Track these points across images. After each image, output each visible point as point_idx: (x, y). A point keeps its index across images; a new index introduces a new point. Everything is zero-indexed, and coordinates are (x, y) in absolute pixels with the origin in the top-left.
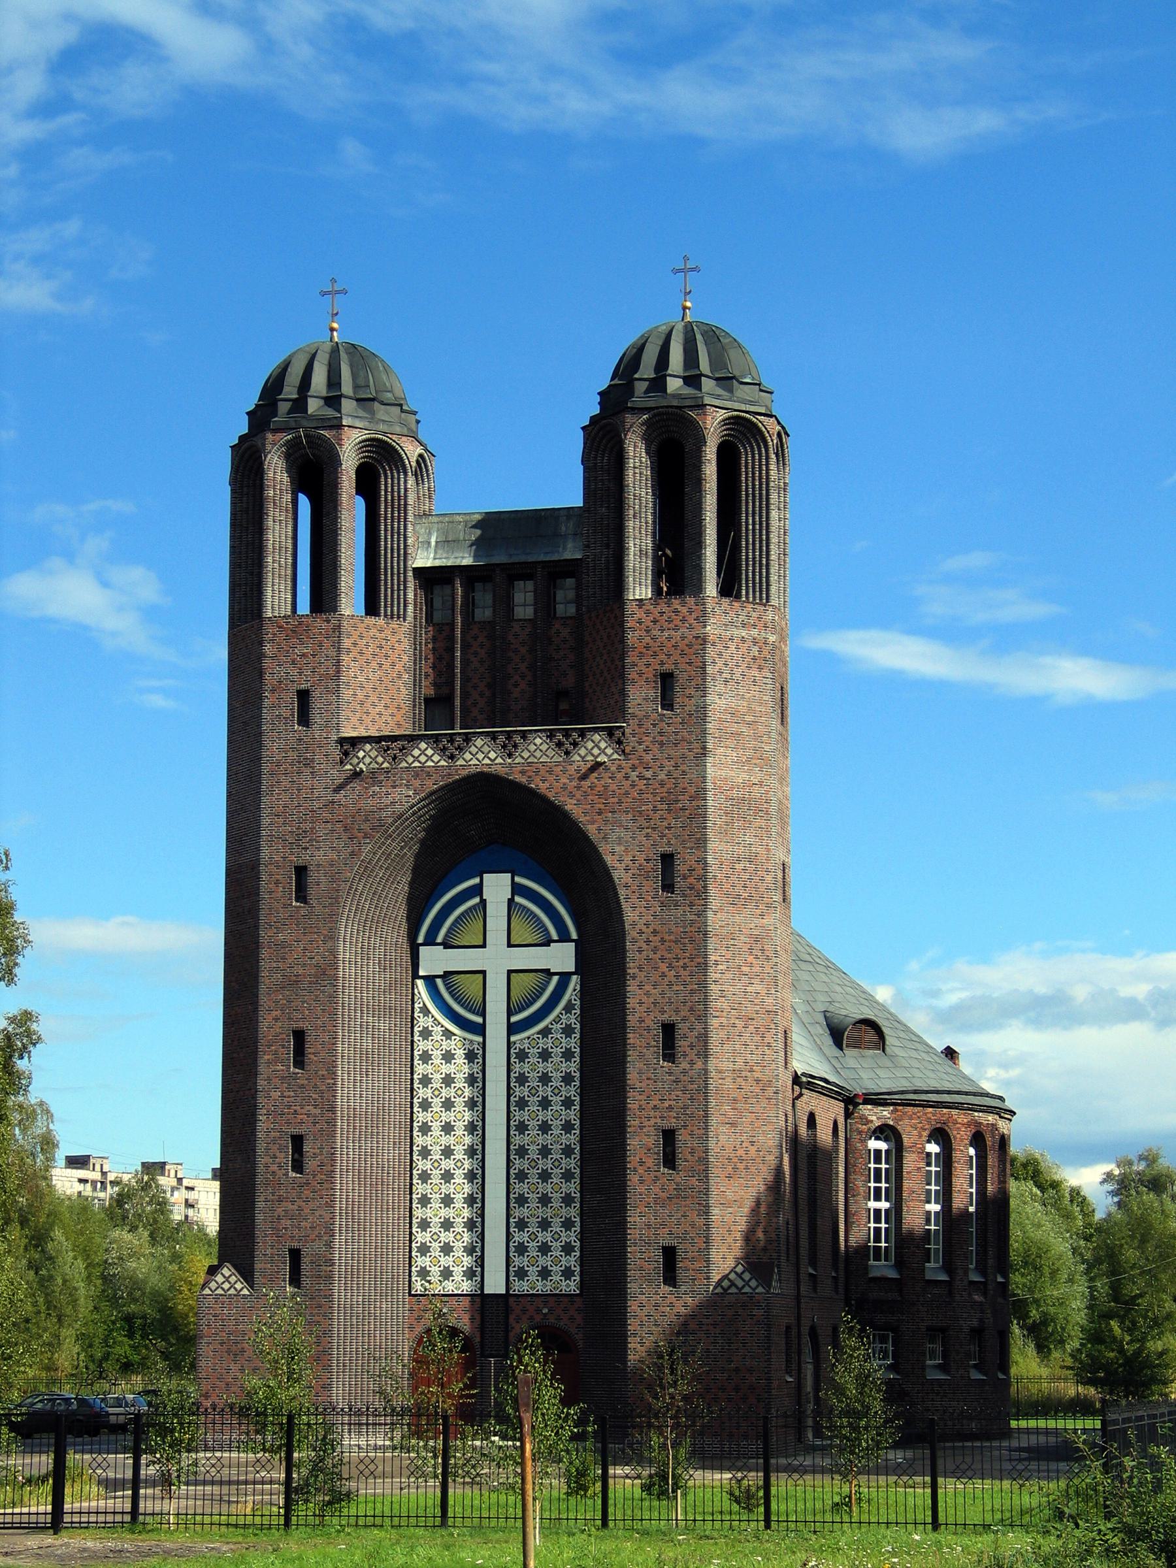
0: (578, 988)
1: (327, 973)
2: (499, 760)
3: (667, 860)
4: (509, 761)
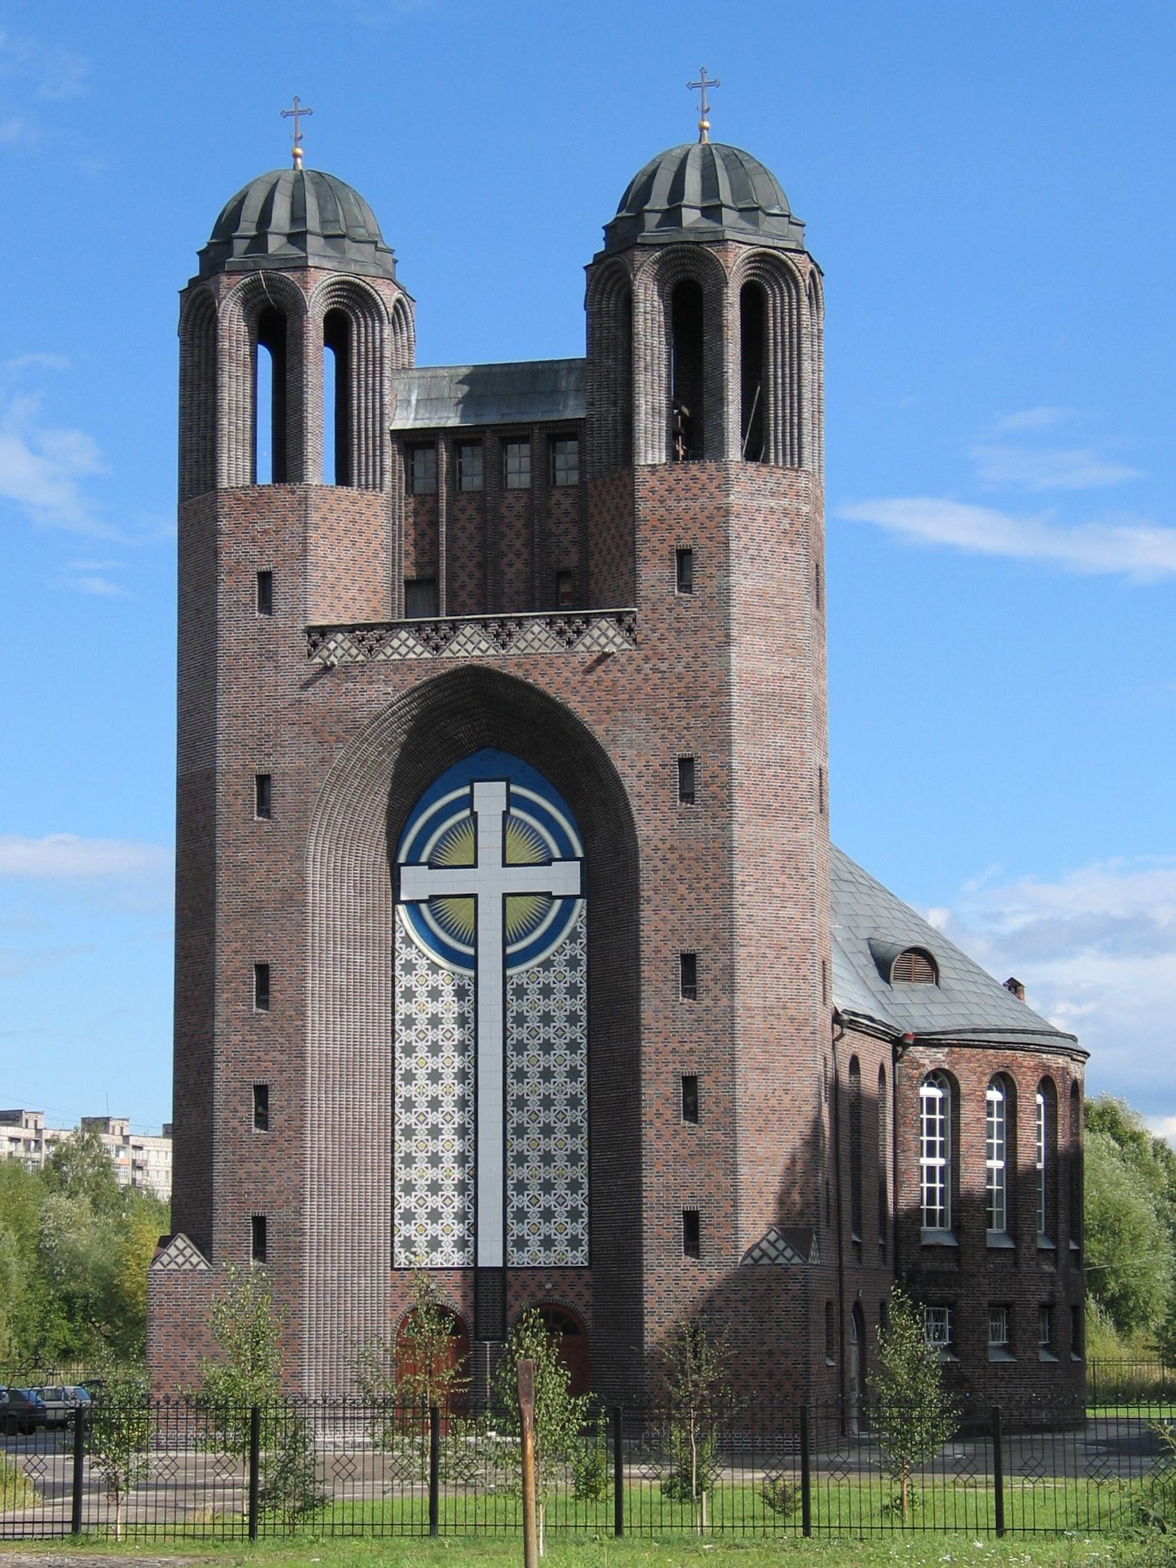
0: (584, 913)
1: (294, 898)
2: (491, 652)
3: (686, 764)
4: (503, 652)
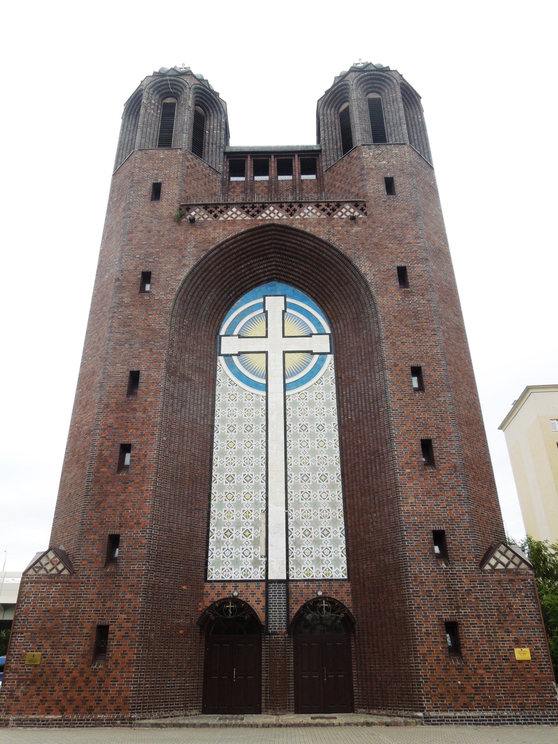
0: (333, 362)
2: (285, 217)
4: (291, 217)
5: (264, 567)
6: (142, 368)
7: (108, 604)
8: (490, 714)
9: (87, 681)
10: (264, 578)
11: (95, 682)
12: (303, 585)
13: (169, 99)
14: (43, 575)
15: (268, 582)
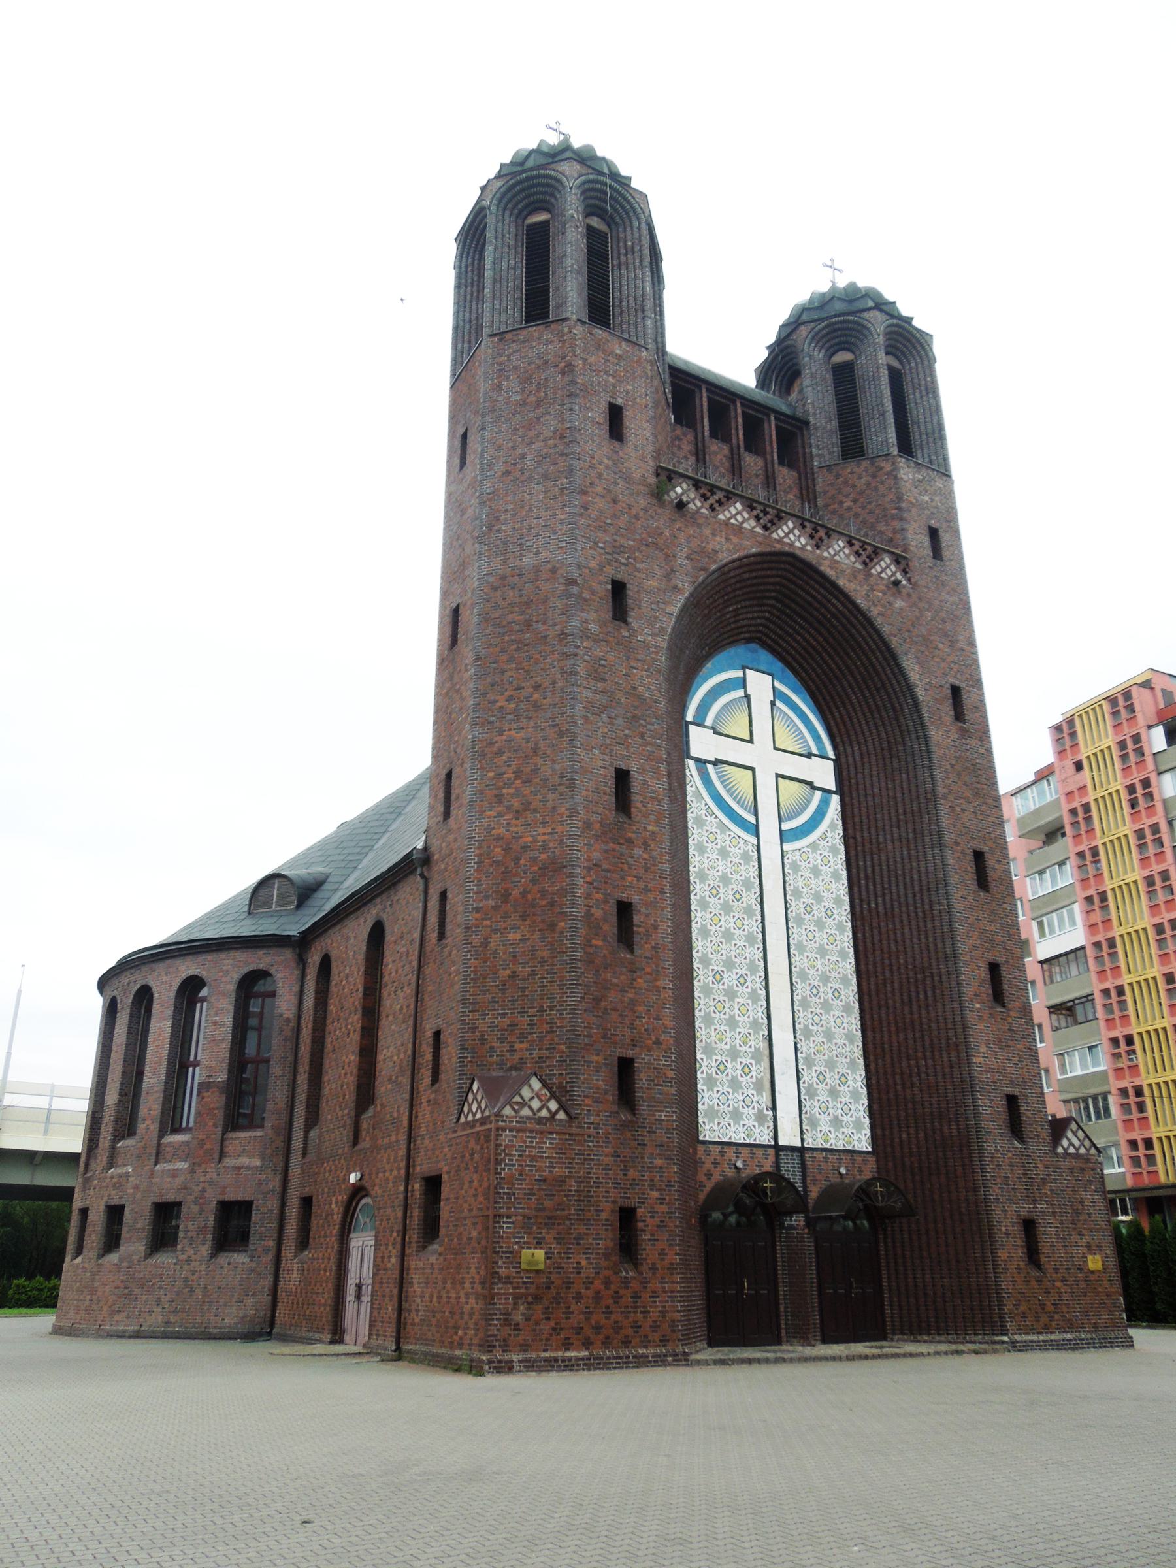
2: (809, 548)
5: (771, 1125)
6: (633, 767)
7: (632, 1173)
8: (1068, 1336)
9: (617, 1297)
10: (773, 1143)
11: (627, 1299)
12: (716, 1149)
13: (596, 219)
14: (528, 1118)
15: (777, 1148)
